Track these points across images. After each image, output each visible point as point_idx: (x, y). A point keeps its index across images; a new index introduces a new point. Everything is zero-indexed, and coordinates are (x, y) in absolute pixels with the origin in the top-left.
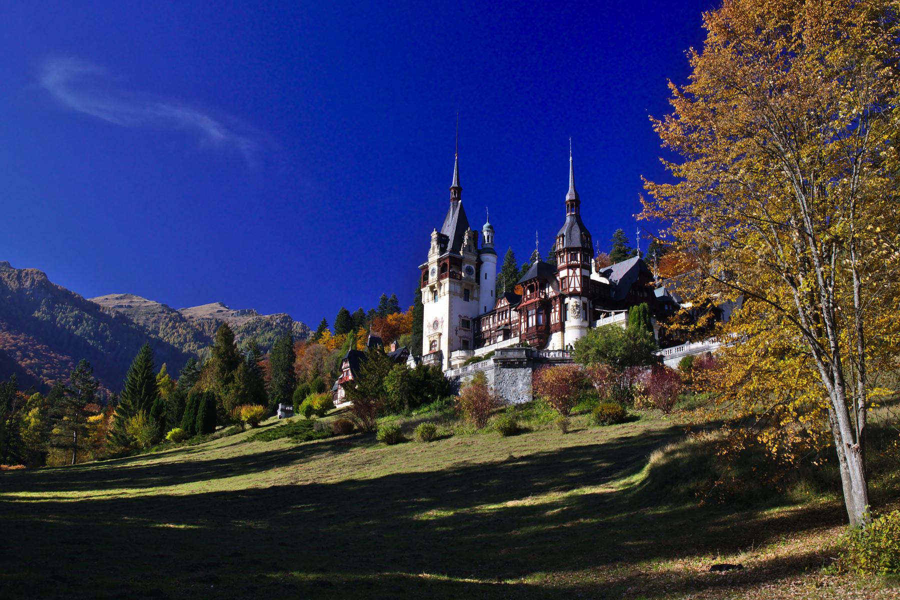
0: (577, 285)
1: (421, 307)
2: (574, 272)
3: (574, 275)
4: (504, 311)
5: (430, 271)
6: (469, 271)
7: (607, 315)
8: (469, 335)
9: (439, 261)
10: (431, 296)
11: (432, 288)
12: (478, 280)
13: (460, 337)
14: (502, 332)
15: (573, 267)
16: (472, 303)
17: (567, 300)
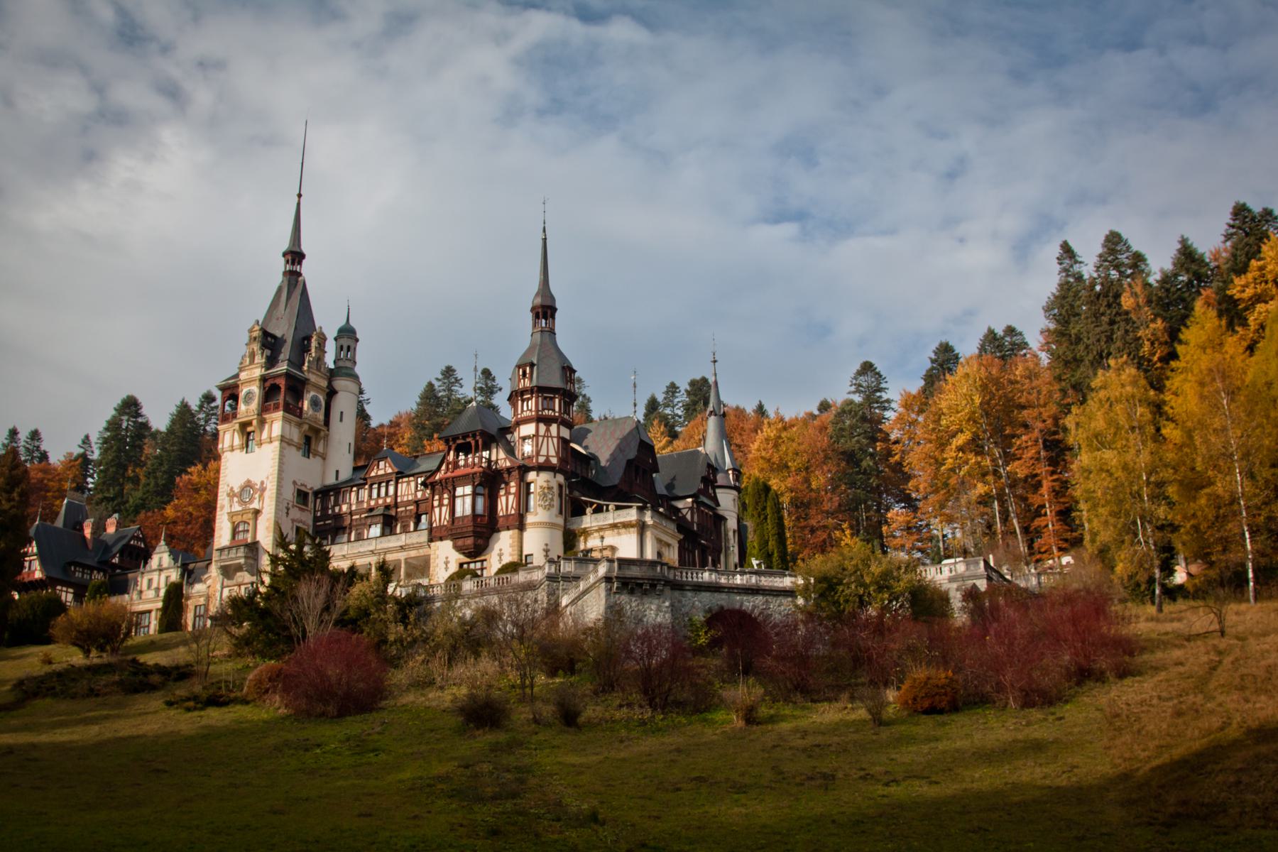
0: (552, 452)
1: (217, 458)
2: (548, 430)
3: (548, 435)
4: (384, 480)
5: (242, 395)
6: (315, 403)
7: (599, 510)
8: (307, 519)
9: (264, 379)
10: (237, 441)
11: (243, 426)
12: (327, 422)
13: (293, 521)
14: (381, 519)
15: (548, 421)
16: (315, 462)
17: (532, 476)
